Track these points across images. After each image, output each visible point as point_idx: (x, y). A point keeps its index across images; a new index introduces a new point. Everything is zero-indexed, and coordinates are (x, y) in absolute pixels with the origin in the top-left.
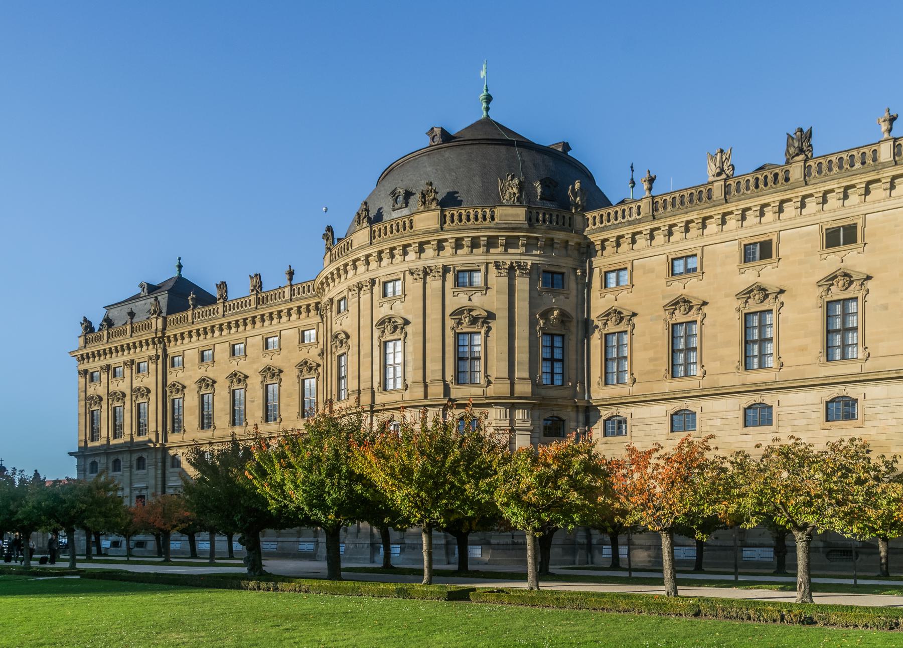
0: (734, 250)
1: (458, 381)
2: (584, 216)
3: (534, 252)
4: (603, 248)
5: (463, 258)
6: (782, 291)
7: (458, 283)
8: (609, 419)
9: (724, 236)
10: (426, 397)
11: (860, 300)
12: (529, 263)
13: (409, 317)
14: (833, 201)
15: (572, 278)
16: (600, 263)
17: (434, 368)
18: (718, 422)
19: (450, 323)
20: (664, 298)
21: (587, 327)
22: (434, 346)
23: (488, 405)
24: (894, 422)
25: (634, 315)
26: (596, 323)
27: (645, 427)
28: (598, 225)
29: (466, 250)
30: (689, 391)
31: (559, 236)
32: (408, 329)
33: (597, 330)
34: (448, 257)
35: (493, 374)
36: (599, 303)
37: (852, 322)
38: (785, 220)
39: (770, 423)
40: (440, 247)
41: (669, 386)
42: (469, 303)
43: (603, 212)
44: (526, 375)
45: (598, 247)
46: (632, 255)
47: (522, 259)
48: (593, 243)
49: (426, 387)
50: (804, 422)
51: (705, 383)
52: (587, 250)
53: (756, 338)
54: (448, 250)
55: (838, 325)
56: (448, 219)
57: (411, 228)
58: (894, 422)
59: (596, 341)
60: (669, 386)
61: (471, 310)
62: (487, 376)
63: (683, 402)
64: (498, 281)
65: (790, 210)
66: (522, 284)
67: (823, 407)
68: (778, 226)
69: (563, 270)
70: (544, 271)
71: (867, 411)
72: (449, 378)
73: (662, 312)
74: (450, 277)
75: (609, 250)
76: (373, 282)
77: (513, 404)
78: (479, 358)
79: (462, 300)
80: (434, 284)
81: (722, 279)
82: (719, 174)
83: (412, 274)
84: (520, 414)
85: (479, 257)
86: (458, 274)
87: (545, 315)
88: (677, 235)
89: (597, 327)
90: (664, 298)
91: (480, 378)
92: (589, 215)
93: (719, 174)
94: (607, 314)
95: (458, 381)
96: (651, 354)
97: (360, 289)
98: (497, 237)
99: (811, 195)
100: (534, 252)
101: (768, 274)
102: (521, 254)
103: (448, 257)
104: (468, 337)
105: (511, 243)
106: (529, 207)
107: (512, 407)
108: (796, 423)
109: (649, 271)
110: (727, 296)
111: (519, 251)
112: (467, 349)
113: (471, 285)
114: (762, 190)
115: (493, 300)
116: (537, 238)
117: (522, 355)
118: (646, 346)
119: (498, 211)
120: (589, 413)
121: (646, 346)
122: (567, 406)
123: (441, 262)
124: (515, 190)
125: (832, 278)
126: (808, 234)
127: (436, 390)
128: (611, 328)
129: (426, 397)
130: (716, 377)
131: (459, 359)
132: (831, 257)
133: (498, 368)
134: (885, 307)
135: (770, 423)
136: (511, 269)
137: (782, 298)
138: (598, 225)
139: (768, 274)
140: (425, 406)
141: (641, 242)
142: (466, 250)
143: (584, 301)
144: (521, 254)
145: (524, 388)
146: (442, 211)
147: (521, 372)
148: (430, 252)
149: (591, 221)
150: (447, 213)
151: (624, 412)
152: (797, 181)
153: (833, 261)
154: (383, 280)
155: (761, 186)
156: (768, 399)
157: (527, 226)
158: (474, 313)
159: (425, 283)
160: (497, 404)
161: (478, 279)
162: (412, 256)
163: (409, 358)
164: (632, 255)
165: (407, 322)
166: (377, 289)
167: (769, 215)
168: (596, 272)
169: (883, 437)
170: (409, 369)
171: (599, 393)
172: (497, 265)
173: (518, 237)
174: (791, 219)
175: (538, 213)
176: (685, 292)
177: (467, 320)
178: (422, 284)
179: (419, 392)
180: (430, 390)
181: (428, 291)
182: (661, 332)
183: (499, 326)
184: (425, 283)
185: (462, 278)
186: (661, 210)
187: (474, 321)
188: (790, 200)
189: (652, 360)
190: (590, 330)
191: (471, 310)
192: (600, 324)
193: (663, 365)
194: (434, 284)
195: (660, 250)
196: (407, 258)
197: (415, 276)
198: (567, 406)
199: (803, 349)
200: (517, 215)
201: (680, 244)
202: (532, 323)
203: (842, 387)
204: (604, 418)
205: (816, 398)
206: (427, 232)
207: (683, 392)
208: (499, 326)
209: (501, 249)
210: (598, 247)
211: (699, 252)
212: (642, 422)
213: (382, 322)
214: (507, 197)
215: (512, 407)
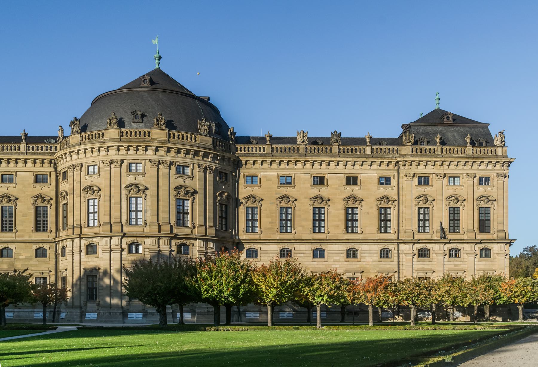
0: (309, 178)
1: (178, 224)
2: (235, 146)
3: (216, 162)
4: (246, 164)
5: (181, 159)
6: (329, 200)
7: (178, 172)
8: (248, 250)
9: (304, 171)
10: (160, 232)
11: (359, 208)
12: (214, 167)
13: (148, 186)
14: (349, 165)
15: (231, 176)
16: (244, 171)
17: (164, 216)
18: (302, 255)
19: (173, 193)
20: (276, 194)
21: (237, 203)
22: (164, 205)
23: (195, 239)
24: (372, 260)
25: (262, 200)
26: (242, 200)
27: (268, 255)
28: (243, 152)
29: (182, 155)
30: (290, 240)
31: (227, 155)
32: (147, 192)
33: (242, 205)
34: (172, 156)
35: (197, 222)
36: (243, 191)
37: (356, 217)
38: (331, 169)
39: (324, 257)
40: (168, 151)
41: (279, 236)
42: (184, 184)
43: (246, 146)
44: (212, 224)
45: (244, 163)
46: (261, 171)
47: (211, 164)
48: (241, 161)
49: (160, 226)
50: (338, 258)
51: (296, 236)
52: (238, 164)
53: (317, 218)
54: (173, 153)
55: (350, 218)
56: (172, 136)
57: (149, 136)
58: (372, 260)
59: (241, 210)
60: (279, 236)
61: (185, 187)
62: (193, 223)
63: (286, 244)
64: (198, 174)
65: (332, 165)
66: (210, 177)
67: (345, 252)
68: (327, 171)
69: (227, 172)
70: (220, 172)
71: (362, 255)
72: (173, 221)
73: (275, 201)
74: (173, 168)
75: (249, 165)
76: (122, 162)
77: (207, 239)
78: (188, 213)
79: (179, 181)
80: (163, 170)
81: (303, 191)
82: (302, 142)
83: (151, 162)
84: (210, 245)
85: (189, 160)
86: (178, 167)
87: (221, 195)
88: (283, 166)
89: (242, 203)
90: (276, 194)
91: (189, 224)
92: (238, 146)
93: (302, 142)
94: (248, 197)
95: (178, 224)
96: (270, 220)
97: (111, 163)
98: (200, 151)
99: (342, 161)
100: (216, 162)
101: (323, 191)
102: (210, 162)
103: (172, 156)
104: (181, 201)
105: (206, 155)
106: (213, 138)
107: (206, 241)
108: (335, 258)
109: (269, 180)
110: (305, 198)
111: (209, 160)
112: (181, 208)
113: (184, 174)
114: (321, 154)
115: (196, 184)
116: (218, 155)
117: (210, 214)
118: (267, 216)
119: (198, 137)
120: (239, 245)
121: (267, 216)
122: (229, 242)
123: (168, 159)
124: (206, 128)
125: (349, 198)
126: (339, 177)
127: (166, 229)
128: (250, 204)
129: (160, 232)
130: (301, 234)
131: (178, 213)
132: (348, 189)
133: (199, 220)
134: (368, 213)
135: (324, 257)
136: (206, 169)
137: (329, 203)
138: (243, 152)
139: (323, 191)
140: (160, 237)
141: (265, 165)
142: (191, 156)
143: (235, 189)
144: (210, 162)
145: (212, 232)
146: (169, 131)
147: (210, 223)
148: (161, 152)
149: (239, 149)
150: (171, 133)
151: (257, 247)
152: (335, 154)
153: (350, 190)
154: (129, 162)
155: (320, 152)
156: (324, 247)
157: (212, 148)
158: (187, 189)
159: (158, 169)
160: (199, 239)
161: (188, 171)
162: (150, 152)
163: (148, 208)
164: (261, 171)
165: (147, 189)
166: (124, 166)
167: (324, 166)
168: (242, 175)
169: (368, 266)
170: (148, 214)
171: (243, 236)
172: (199, 166)
173: (210, 153)
174: (333, 169)
175: (217, 142)
176: (286, 193)
177: (183, 192)
178: (157, 169)
179: (156, 229)
180: (162, 228)
181: (160, 173)
182: (275, 210)
183: (199, 198)
184: (158, 169)
185: (180, 170)
186: (275, 152)
187: (187, 193)
188: (333, 161)
189: (270, 223)
190: (239, 204)
191: (185, 187)
192: (244, 202)
193: (276, 226)
194: (163, 170)
195: (275, 171)
196: (147, 153)
197: (152, 164)
198: (229, 242)
199: (337, 226)
200: (208, 141)
201: (284, 170)
202: (215, 198)
203: (353, 244)
204: (246, 249)
205: (343, 248)
206: (160, 141)
207: (288, 240)
208: (199, 198)
209: (200, 158)
210: (244, 163)
211: (293, 176)
212: (266, 252)
213: (129, 186)
214: (202, 130)
215: (206, 241)
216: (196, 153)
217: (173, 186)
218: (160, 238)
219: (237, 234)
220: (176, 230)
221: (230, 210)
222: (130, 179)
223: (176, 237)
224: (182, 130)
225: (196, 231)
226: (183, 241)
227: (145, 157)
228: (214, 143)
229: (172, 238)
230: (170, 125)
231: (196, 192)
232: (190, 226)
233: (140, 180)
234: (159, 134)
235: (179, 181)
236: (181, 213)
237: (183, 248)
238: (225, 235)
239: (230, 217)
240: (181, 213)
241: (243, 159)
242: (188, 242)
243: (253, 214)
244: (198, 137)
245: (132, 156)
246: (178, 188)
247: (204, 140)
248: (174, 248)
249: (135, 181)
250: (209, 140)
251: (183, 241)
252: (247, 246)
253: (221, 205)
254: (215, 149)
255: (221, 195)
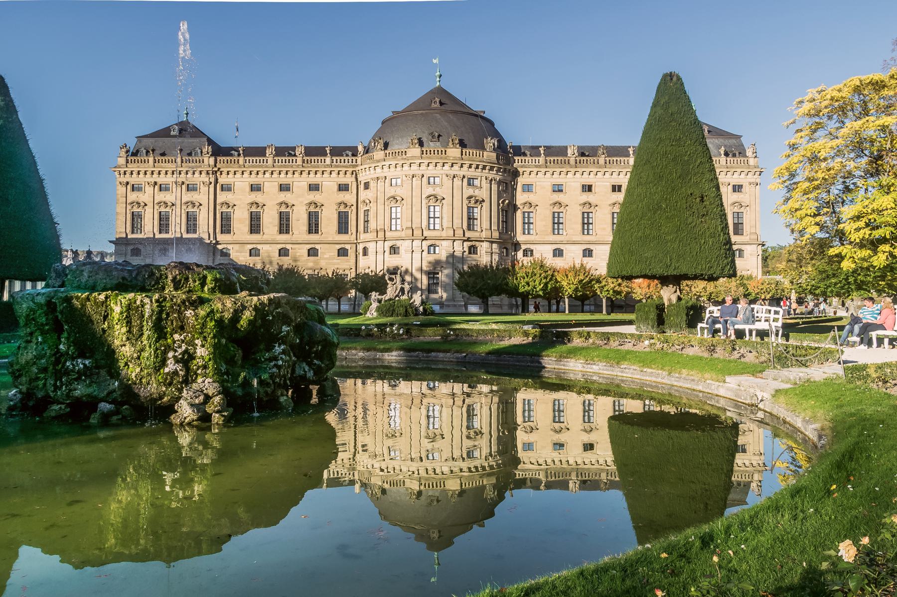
1: (469, 229)
5: (472, 173)
7: (469, 184)
16: (521, 181)
17: (457, 222)
19: (465, 202)
21: (515, 208)
31: (508, 167)
34: (465, 171)
36: (521, 198)
52: (516, 174)
59: (519, 214)
64: (485, 185)
66: (494, 187)
72: (465, 227)
74: (465, 180)
80: (457, 182)
84: (495, 246)
85: (478, 173)
86: (469, 179)
92: (516, 158)
103: (465, 171)
105: (492, 169)
107: (492, 242)
115: (483, 194)
118: (542, 220)
119: (485, 153)
120: (516, 246)
123: (461, 173)
127: (459, 233)
128: (526, 209)
131: (469, 219)
133: (486, 225)
145: (496, 235)
147: (494, 227)
148: (456, 167)
151: (532, 247)
161: (477, 182)
162: (447, 167)
163: (445, 216)
166: (425, 179)
168: (519, 184)
171: (520, 237)
183: (486, 205)
185: (470, 182)
194: (457, 182)
199: (604, 229)
202: (499, 205)
206: (455, 158)
208: (486, 205)
215: (492, 242)
216: (484, 168)
217: (465, 196)
218: (454, 240)
219: (515, 236)
220: (468, 234)
221: (510, 214)
222: (429, 191)
223: (468, 240)
224: (471, 148)
225: (484, 235)
226: (473, 243)
227: (442, 172)
228: (498, 158)
229: (465, 241)
230: (462, 144)
231: (483, 201)
232: (479, 230)
233: (439, 192)
234: (454, 152)
235: (469, 191)
236: (471, 218)
237: (473, 250)
238: (505, 237)
239: (510, 221)
240: (471, 218)
241: (521, 170)
242: (477, 244)
243: (529, 217)
244: (485, 153)
245: (431, 171)
246: (470, 198)
247: (490, 155)
248: (466, 249)
249: (433, 193)
250: (494, 155)
251: (473, 243)
252: (523, 247)
253: (503, 210)
254: (498, 163)
255: (503, 202)
